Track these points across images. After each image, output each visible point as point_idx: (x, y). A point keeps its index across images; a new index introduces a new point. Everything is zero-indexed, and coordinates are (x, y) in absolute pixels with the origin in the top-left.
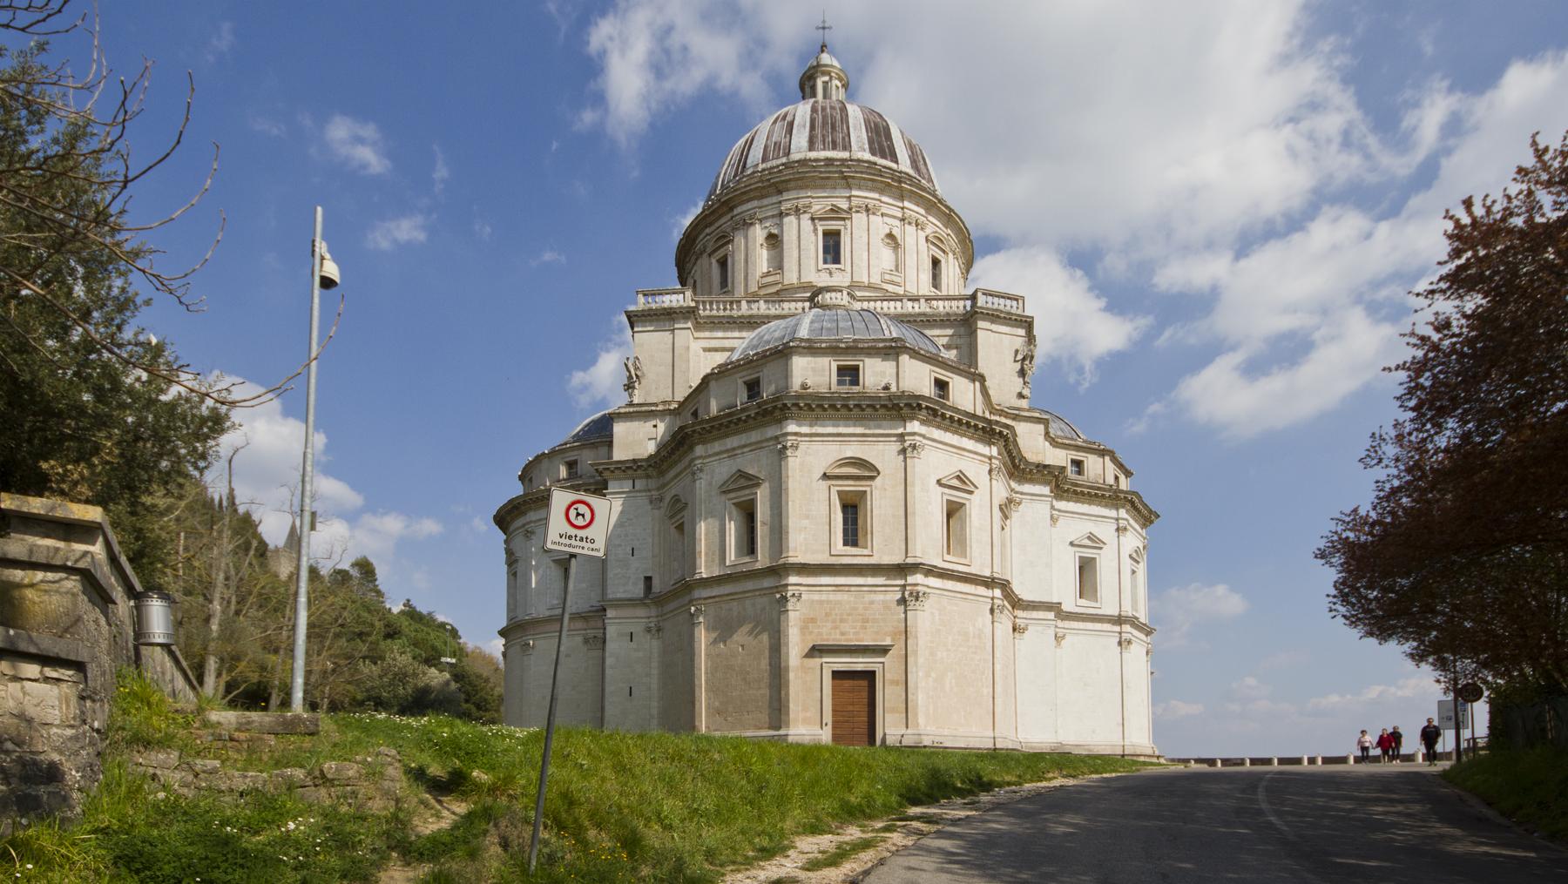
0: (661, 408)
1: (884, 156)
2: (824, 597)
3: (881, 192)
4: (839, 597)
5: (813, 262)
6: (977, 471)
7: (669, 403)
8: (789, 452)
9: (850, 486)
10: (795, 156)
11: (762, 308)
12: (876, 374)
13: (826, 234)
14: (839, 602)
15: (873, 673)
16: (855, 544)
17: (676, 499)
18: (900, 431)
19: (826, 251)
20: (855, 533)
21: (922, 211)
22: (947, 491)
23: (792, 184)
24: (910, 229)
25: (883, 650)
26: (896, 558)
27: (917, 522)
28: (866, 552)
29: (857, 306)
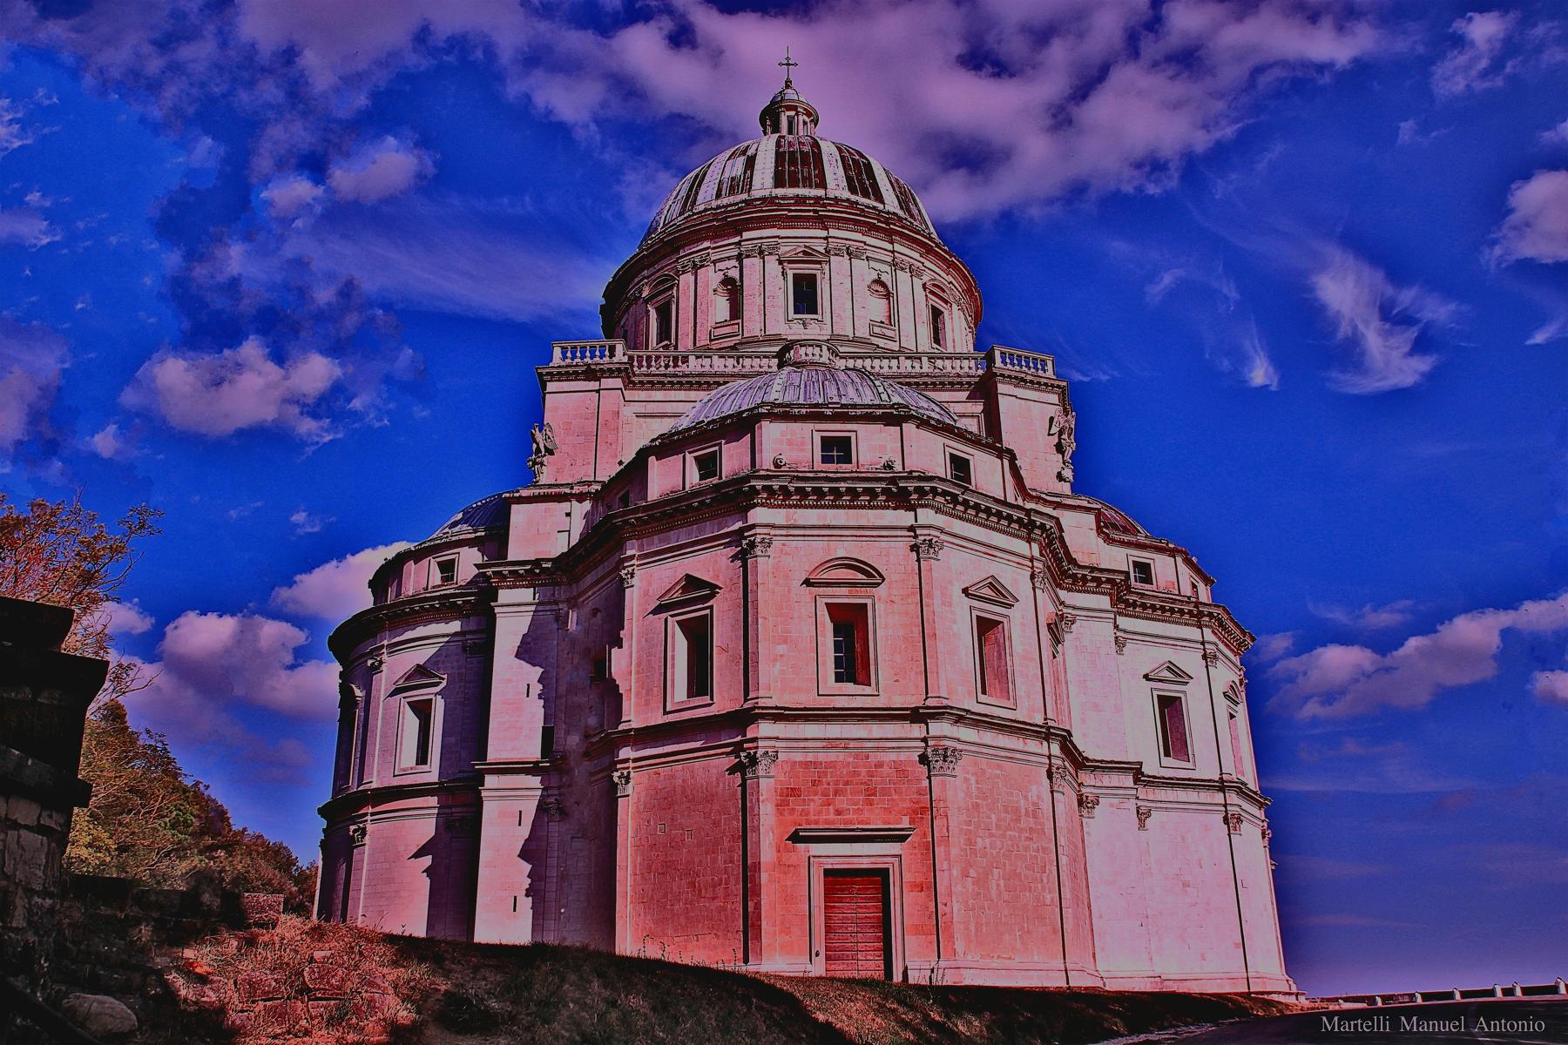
0: (576, 490)
1: (866, 195)
2: (810, 757)
4: (832, 756)
5: (781, 311)
6: (1016, 579)
7: (589, 483)
8: (758, 551)
9: (842, 596)
10: (756, 194)
11: (718, 364)
12: (874, 447)
14: (831, 765)
15: (883, 874)
22: (976, 603)
24: (903, 276)
26: (914, 701)
27: (940, 647)
28: (868, 690)
29: (841, 364)
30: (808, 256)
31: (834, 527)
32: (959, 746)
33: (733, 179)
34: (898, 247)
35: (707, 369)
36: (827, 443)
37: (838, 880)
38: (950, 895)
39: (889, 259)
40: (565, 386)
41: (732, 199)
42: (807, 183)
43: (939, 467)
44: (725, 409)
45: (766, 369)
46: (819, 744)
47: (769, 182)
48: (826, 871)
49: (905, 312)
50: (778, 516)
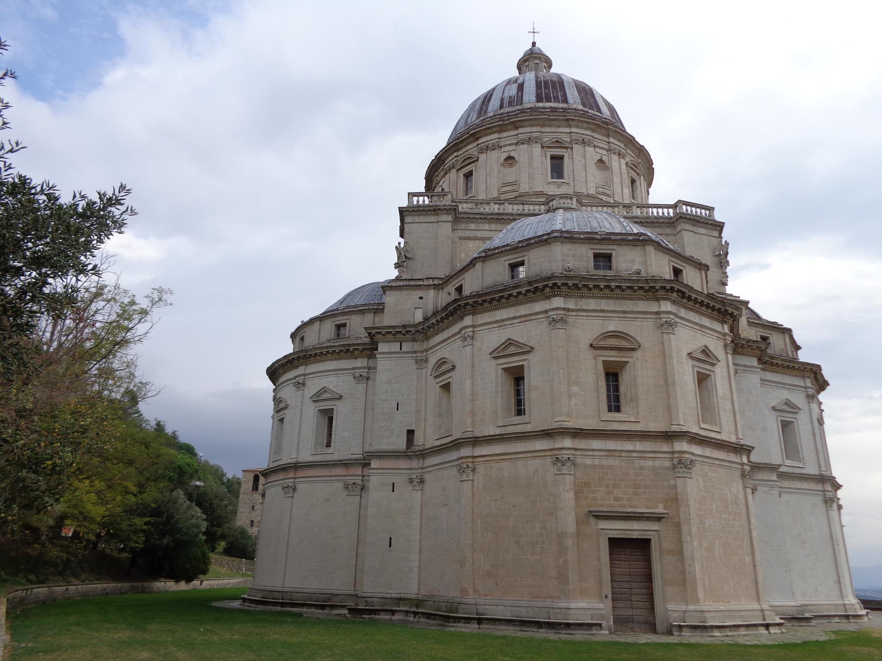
2: (596, 462)
3: (593, 131)
4: (611, 462)
6: (717, 347)
9: (613, 357)
13: (553, 158)
16: (618, 409)
17: (442, 362)
18: (656, 310)
19: (553, 171)
20: (617, 399)
21: (622, 146)
22: (696, 363)
23: (527, 123)
24: (615, 158)
25: (658, 518)
30: (559, 144)
31: (607, 311)
32: (693, 458)
33: (510, 97)
34: (611, 140)
35: (502, 211)
36: (596, 256)
37: (616, 544)
38: (693, 559)
39: (607, 147)
40: (417, 219)
41: (511, 109)
42: (556, 100)
43: (668, 275)
44: (525, 234)
45: (537, 212)
46: (602, 453)
47: (534, 98)
48: (610, 539)
49: (616, 179)
50: (571, 304)
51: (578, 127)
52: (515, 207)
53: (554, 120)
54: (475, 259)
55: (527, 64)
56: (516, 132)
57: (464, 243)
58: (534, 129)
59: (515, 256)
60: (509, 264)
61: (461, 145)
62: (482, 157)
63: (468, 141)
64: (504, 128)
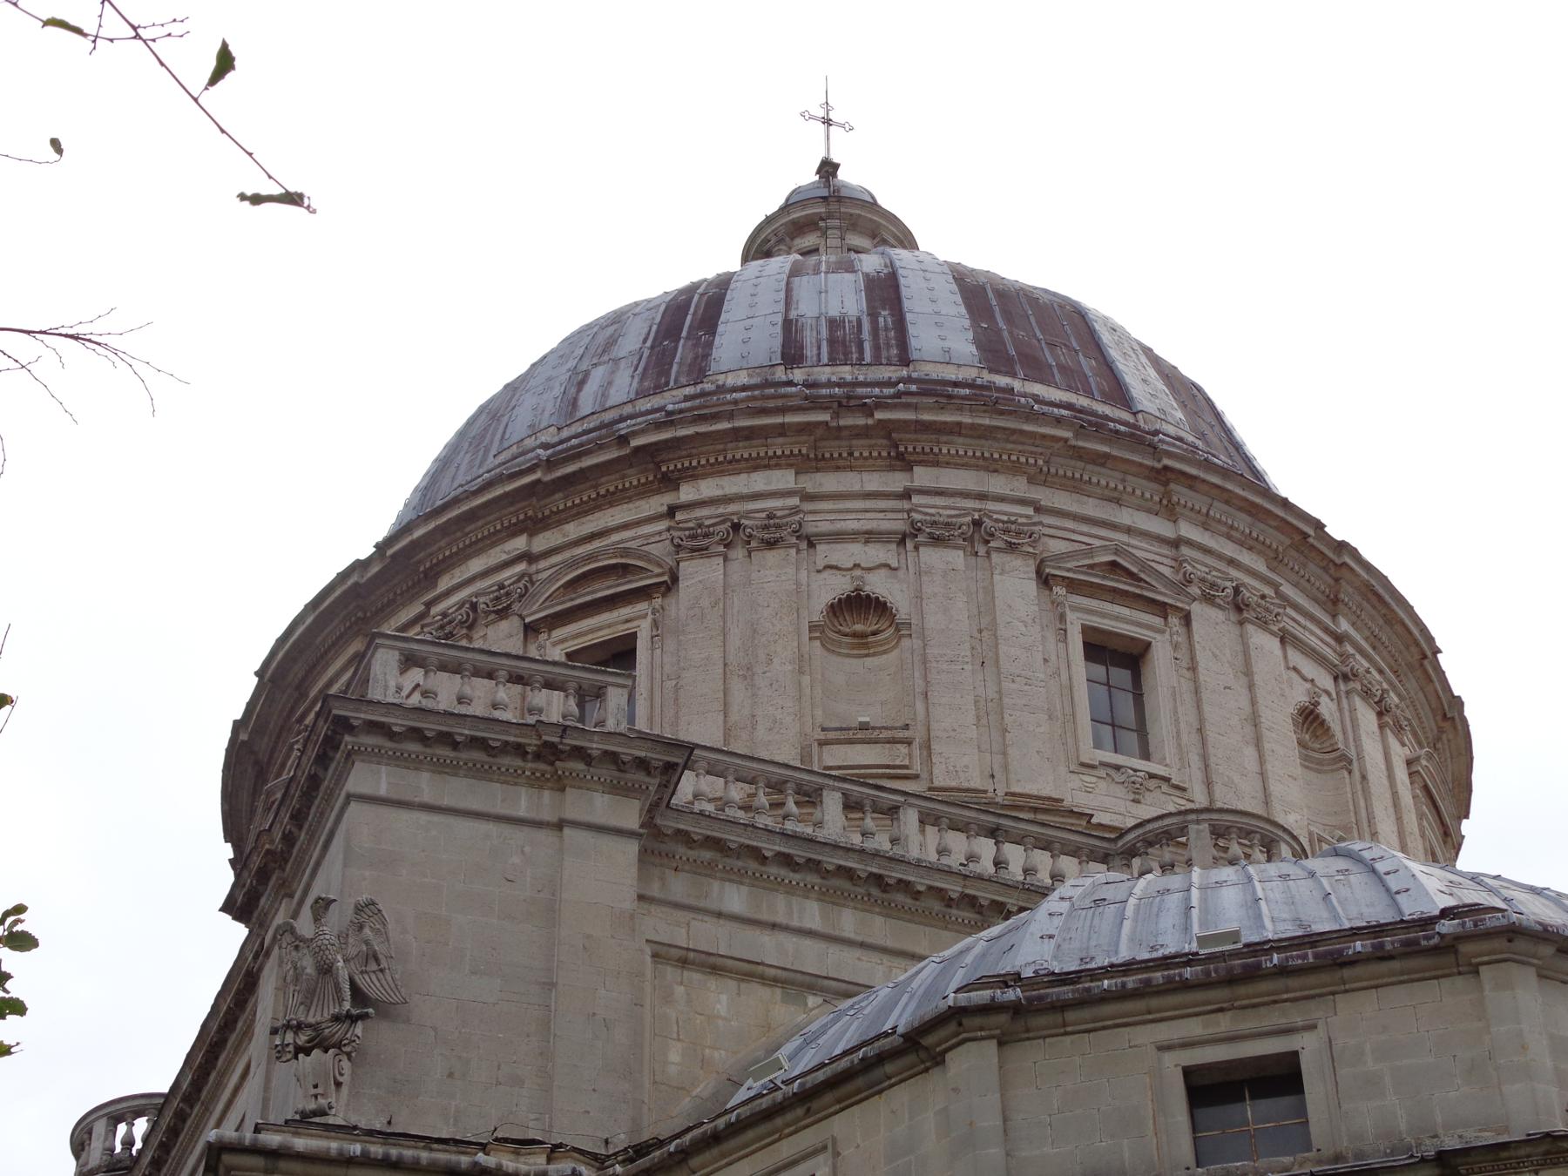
23: (960, 446)
33: (834, 324)
51: (1206, 524)
52: (958, 844)
53: (1101, 460)
54: (956, 1014)
55: (809, 240)
56: (897, 481)
57: (683, 985)
58: (998, 484)
59: (1225, 1023)
60: (1188, 1072)
61: (559, 501)
62: (699, 575)
63: (609, 484)
64: (832, 448)
